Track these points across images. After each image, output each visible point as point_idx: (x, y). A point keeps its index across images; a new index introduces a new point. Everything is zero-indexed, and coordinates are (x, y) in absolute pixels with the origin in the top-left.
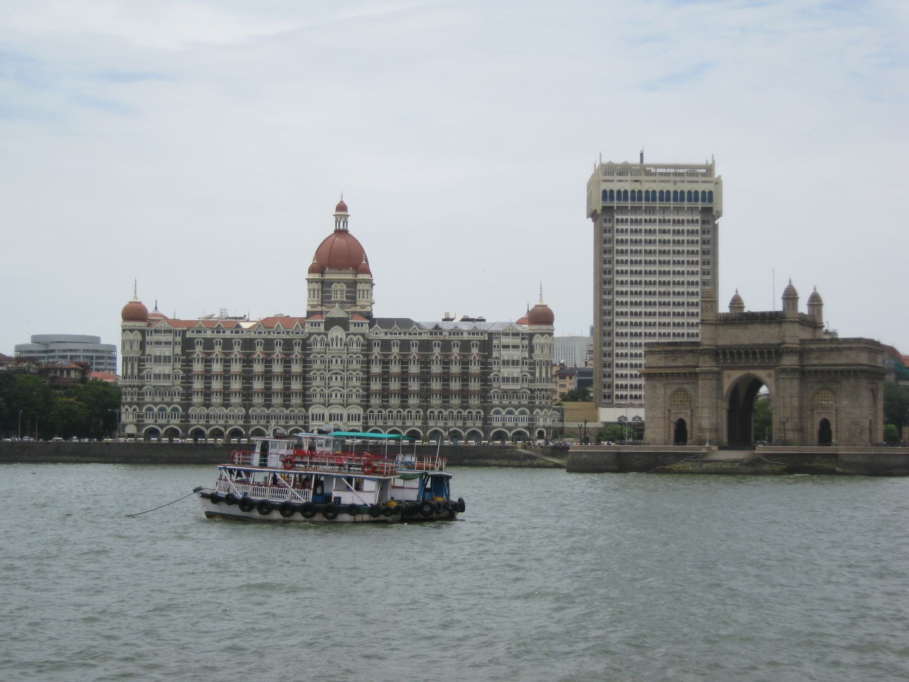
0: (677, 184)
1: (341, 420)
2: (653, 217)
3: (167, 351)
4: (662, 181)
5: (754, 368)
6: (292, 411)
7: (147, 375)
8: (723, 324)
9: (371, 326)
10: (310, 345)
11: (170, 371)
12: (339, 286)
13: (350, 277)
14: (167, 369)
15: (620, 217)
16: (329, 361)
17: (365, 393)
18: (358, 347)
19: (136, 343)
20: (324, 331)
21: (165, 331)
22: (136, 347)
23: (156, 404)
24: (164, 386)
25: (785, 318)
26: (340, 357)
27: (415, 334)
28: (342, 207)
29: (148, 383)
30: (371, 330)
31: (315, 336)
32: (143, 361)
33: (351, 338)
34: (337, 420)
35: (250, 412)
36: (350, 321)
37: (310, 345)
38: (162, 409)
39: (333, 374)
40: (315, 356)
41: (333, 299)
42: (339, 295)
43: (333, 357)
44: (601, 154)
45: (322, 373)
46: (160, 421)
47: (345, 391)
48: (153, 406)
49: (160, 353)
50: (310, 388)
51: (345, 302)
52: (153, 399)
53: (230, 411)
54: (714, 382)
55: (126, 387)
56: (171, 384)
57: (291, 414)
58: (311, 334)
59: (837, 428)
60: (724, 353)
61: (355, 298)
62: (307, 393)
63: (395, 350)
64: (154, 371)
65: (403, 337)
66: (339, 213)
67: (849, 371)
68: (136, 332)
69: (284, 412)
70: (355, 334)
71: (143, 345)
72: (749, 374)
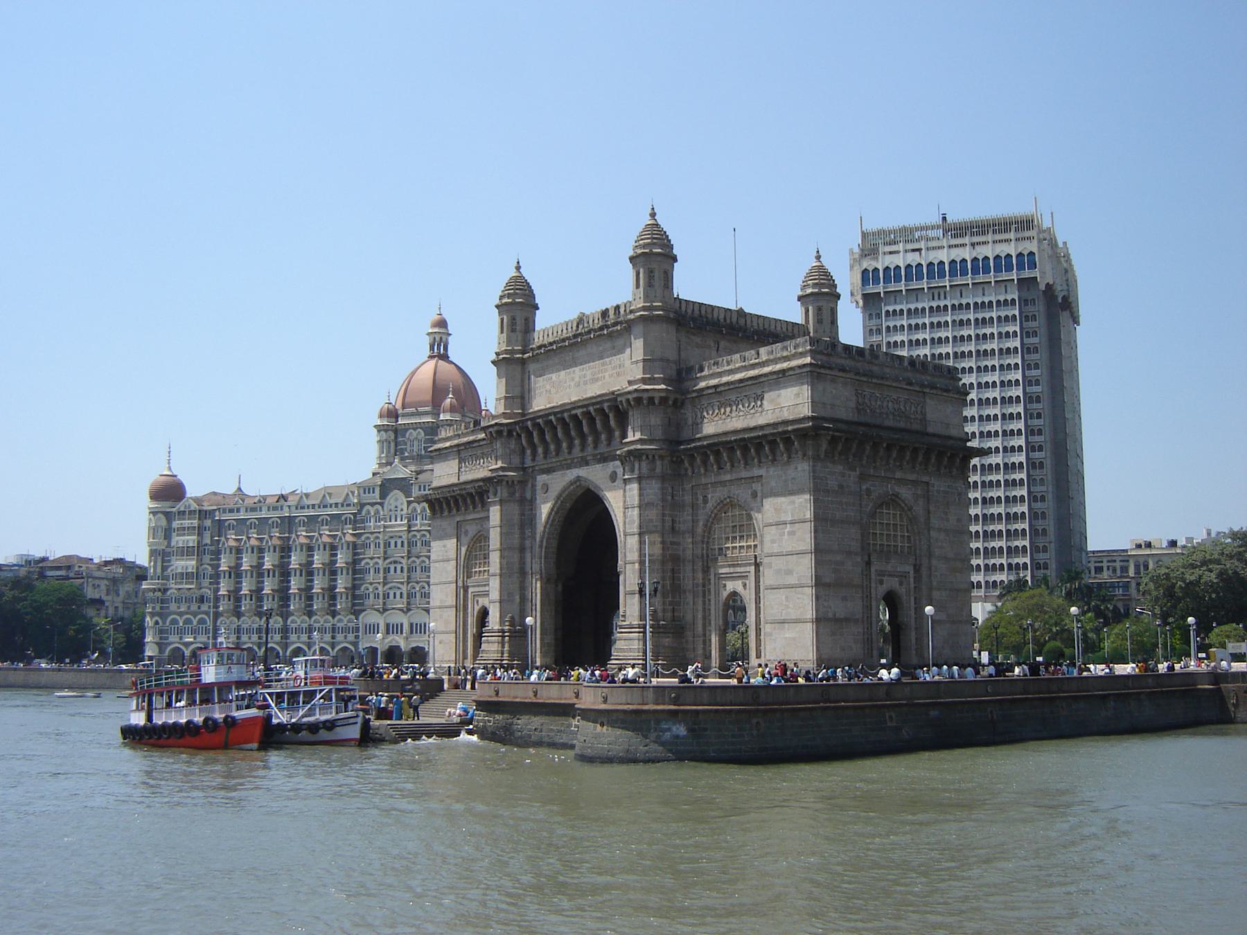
0: (976, 247)
1: (402, 633)
2: (942, 304)
3: (192, 540)
4: (956, 246)
5: (585, 462)
6: (340, 621)
12: (415, 433)
14: (190, 564)
15: (891, 309)
16: (385, 544)
22: (161, 534)
23: (181, 614)
26: (400, 537)
29: (173, 586)
31: (368, 507)
32: (169, 554)
35: (289, 623)
38: (188, 621)
39: (391, 563)
40: (368, 538)
42: (415, 449)
43: (392, 537)
44: (861, 218)
45: (377, 563)
47: (404, 589)
48: (178, 617)
54: (515, 509)
57: (338, 624)
62: (357, 592)
66: (436, 330)
68: (160, 515)
72: (578, 478)
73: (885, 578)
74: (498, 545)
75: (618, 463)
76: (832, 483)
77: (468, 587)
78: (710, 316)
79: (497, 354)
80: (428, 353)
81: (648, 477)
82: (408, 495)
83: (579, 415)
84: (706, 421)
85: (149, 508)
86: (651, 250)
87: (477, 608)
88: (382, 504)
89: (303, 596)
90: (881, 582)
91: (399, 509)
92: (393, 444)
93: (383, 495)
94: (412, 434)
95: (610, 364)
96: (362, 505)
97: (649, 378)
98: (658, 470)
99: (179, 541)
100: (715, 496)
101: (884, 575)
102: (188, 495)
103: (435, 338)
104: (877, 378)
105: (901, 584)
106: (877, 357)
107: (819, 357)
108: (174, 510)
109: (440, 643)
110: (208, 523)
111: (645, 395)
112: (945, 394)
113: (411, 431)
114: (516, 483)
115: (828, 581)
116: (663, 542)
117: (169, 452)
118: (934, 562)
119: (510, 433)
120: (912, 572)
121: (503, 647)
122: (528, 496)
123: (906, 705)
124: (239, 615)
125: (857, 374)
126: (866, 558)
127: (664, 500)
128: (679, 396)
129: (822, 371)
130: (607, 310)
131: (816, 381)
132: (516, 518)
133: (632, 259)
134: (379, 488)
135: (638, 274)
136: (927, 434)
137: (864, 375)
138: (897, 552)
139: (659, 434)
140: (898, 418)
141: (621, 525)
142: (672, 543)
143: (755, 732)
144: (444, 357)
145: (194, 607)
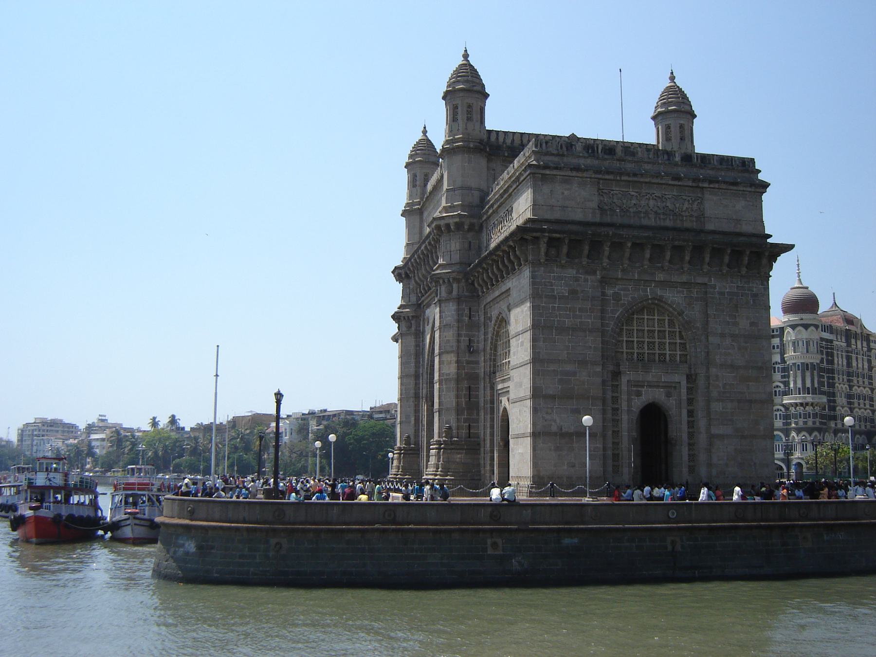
73: (644, 390)
76: (561, 289)
81: (446, 300)
84: (492, 240)
90: (639, 394)
97: (450, 207)
98: (455, 293)
101: (643, 386)
104: (628, 175)
105: (668, 395)
106: (633, 154)
107: (543, 158)
112: (732, 187)
115: (551, 392)
116: (458, 362)
118: (713, 371)
120: (684, 383)
123: (516, 530)
125: (598, 172)
127: (458, 321)
128: (475, 221)
129: (548, 172)
131: (540, 183)
132: (412, 349)
135: (447, 110)
136: (702, 231)
137: (608, 173)
138: (665, 361)
139: (456, 258)
140: (662, 217)
142: (468, 362)
143: (271, 554)
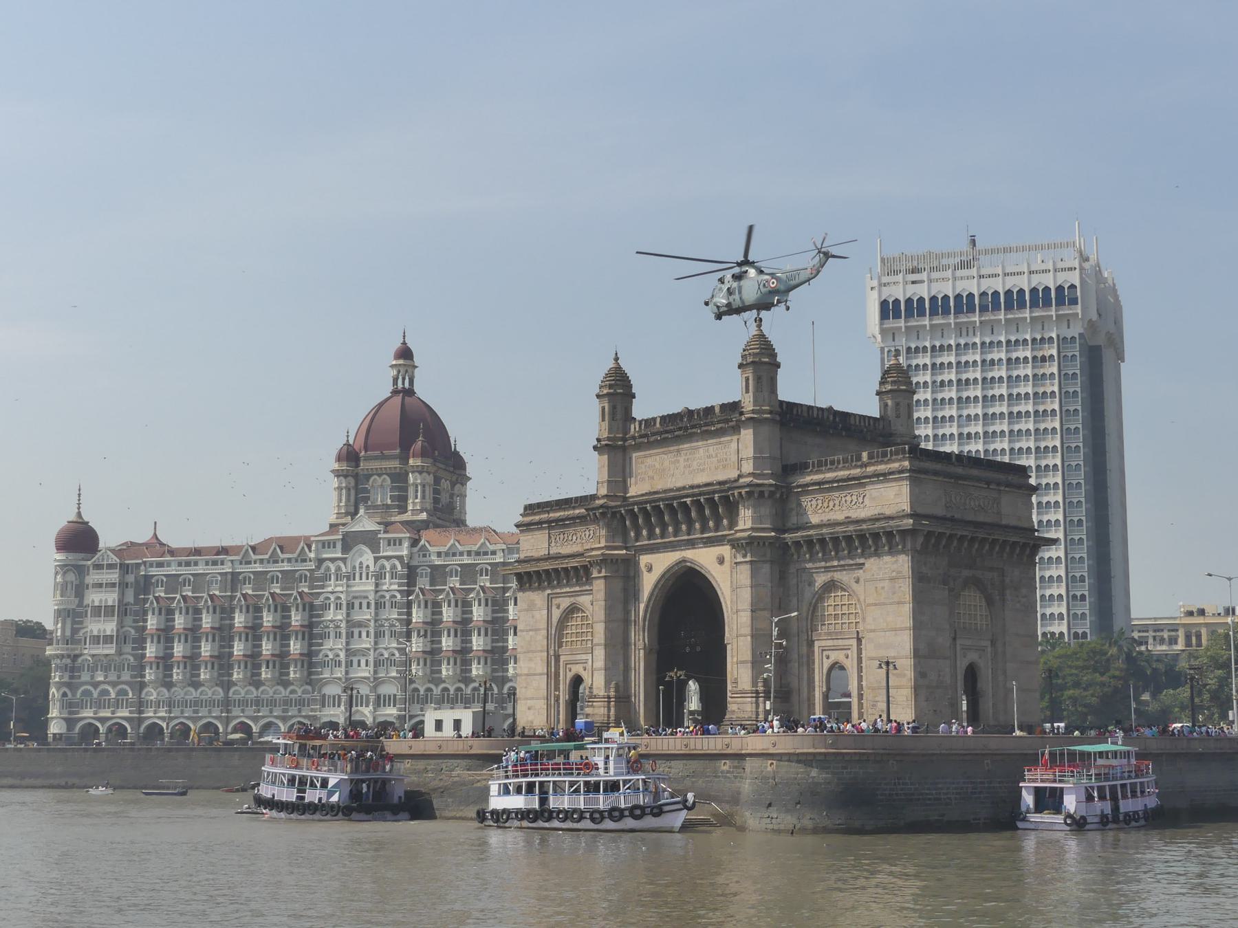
3: (111, 598)
5: (691, 544)
6: (293, 692)
7: (86, 638)
8: (638, 447)
9: (414, 543)
10: (318, 579)
11: (112, 630)
12: (379, 480)
13: (395, 464)
14: (110, 627)
17: (404, 658)
18: (394, 580)
19: (69, 586)
20: (339, 555)
21: (111, 566)
24: (107, 655)
25: (742, 413)
27: (486, 553)
28: (405, 353)
29: (86, 651)
30: (415, 550)
33: (383, 567)
34: (361, 706)
35: (230, 695)
36: (379, 536)
37: (318, 579)
41: (369, 503)
46: (103, 714)
49: (101, 601)
50: (321, 650)
51: (388, 507)
52: (92, 677)
53: (201, 694)
54: (618, 585)
55: (57, 656)
56: (113, 651)
57: (292, 696)
58: (320, 561)
59: (860, 687)
60: (634, 517)
61: (405, 499)
62: (314, 659)
63: (454, 582)
64: (91, 631)
65: (466, 560)
66: (401, 362)
67: (876, 536)
69: (280, 693)
70: (388, 558)
71: (80, 591)
72: (684, 561)
74: (603, 617)
75: (728, 547)
77: (559, 656)
78: (805, 414)
79: (599, 440)
80: (391, 388)
82: (374, 547)
83: (688, 502)
85: (56, 560)
86: (760, 359)
87: (570, 675)
88: (344, 560)
89: (161, 665)
90: (965, 657)
91: (364, 567)
92: (353, 492)
93: (346, 548)
94: (376, 480)
95: (716, 456)
96: (320, 561)
99: (95, 598)
100: (820, 580)
102: (101, 545)
103: (399, 372)
108: (89, 563)
109: (529, 709)
110: (131, 578)
111: (759, 489)
113: (376, 477)
114: (619, 561)
117: (79, 495)
119: (614, 514)
121: (609, 710)
122: (632, 574)
124: (169, 685)
126: (953, 635)
130: (713, 407)
133: (740, 366)
134: (341, 542)
141: (729, 603)
144: (410, 392)
145: (113, 677)
